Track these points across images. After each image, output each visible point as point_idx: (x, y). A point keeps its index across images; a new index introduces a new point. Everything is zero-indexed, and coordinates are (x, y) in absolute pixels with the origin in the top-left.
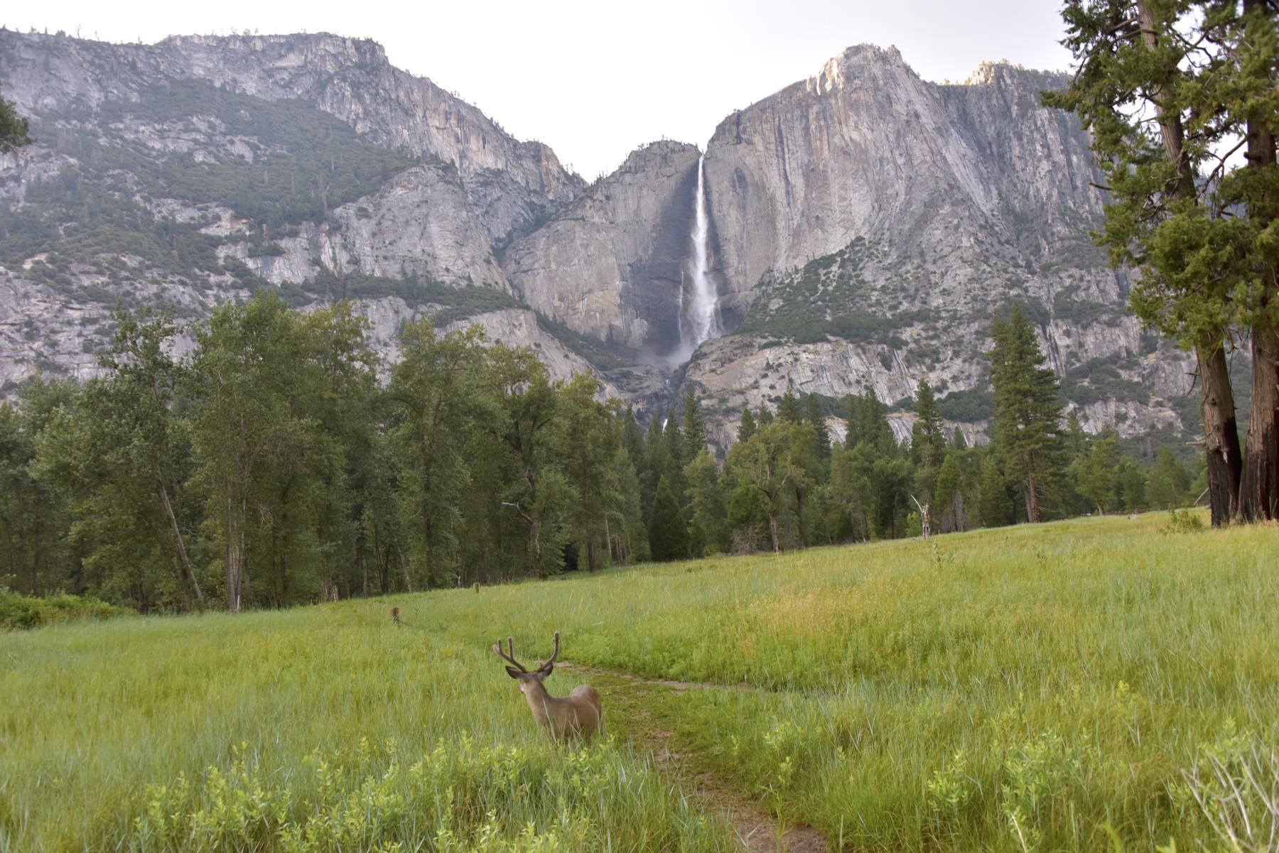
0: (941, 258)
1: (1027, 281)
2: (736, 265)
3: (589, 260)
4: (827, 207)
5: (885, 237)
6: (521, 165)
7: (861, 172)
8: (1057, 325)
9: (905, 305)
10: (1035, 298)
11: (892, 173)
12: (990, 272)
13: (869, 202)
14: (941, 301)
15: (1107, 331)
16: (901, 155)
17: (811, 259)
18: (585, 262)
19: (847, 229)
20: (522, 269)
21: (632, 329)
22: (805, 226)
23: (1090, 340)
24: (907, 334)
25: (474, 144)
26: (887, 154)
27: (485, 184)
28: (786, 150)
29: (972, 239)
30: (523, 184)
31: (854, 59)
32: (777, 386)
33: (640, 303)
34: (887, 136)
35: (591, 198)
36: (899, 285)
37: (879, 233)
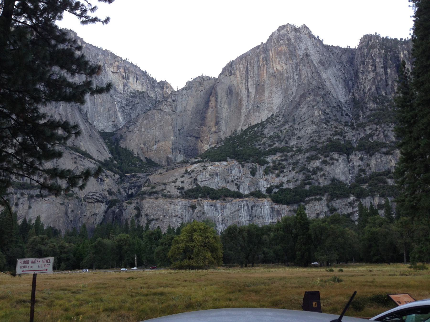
0: (303, 121)
1: (347, 133)
3: (161, 128)
4: (263, 102)
5: (282, 113)
6: (155, 90)
8: (356, 154)
9: (277, 144)
10: (349, 141)
11: (292, 83)
12: (325, 128)
13: (281, 98)
14: (296, 142)
15: (384, 158)
16: (297, 74)
17: (250, 126)
18: (158, 128)
19: (269, 111)
20: (129, 131)
21: (177, 159)
22: (252, 111)
23: (373, 162)
24: (270, 159)
25: (132, 80)
26: (291, 75)
27: (132, 97)
28: (249, 77)
29: (320, 112)
30: (154, 98)
31: (282, 32)
32: (185, 182)
33: (181, 147)
34: (292, 66)
35: (166, 101)
37: (280, 112)
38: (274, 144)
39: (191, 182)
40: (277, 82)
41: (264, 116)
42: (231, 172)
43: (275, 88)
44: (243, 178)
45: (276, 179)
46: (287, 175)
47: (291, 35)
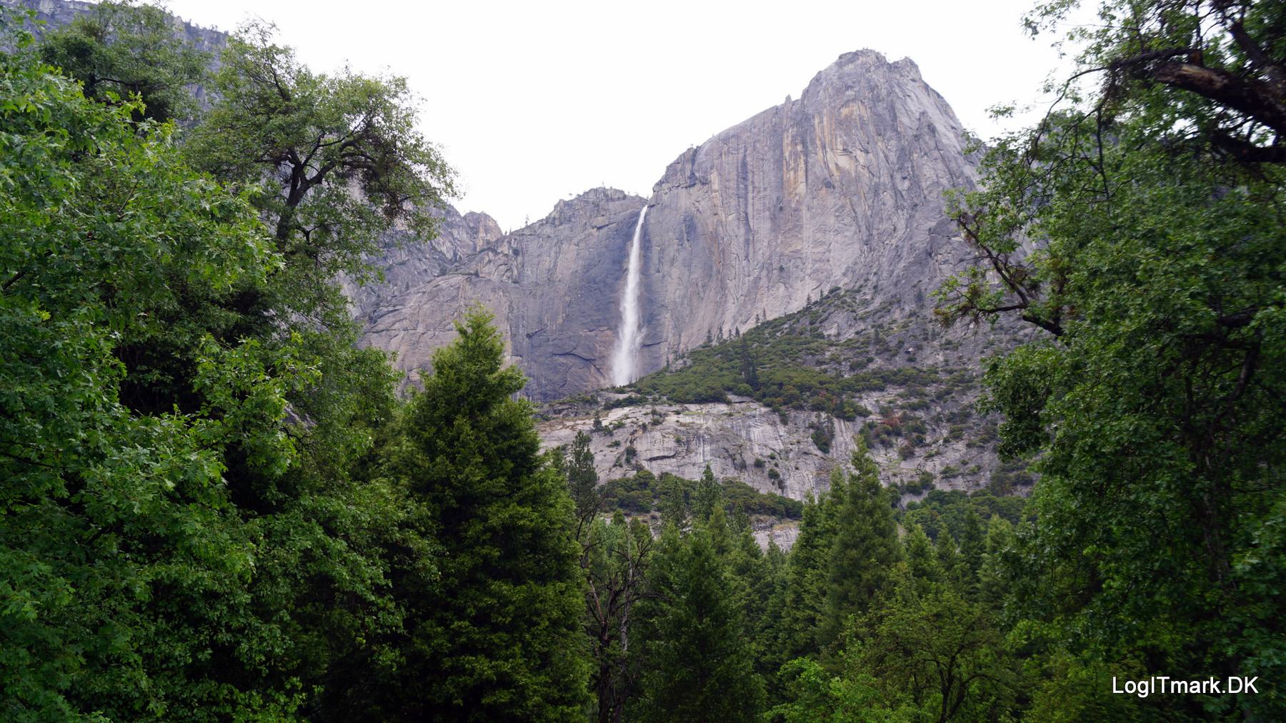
2: (671, 339)
6: (452, 234)
7: (849, 207)
9: (878, 362)
14: (941, 358)
17: (762, 319)
24: (869, 401)
28: (750, 188)
31: (849, 68)
33: (535, 386)
36: (873, 336)
38: (870, 360)
39: (619, 459)
40: (840, 203)
41: (802, 294)
42: (748, 433)
43: (832, 220)
44: (791, 455)
45: (903, 464)
46: (938, 453)
47: (878, 77)
